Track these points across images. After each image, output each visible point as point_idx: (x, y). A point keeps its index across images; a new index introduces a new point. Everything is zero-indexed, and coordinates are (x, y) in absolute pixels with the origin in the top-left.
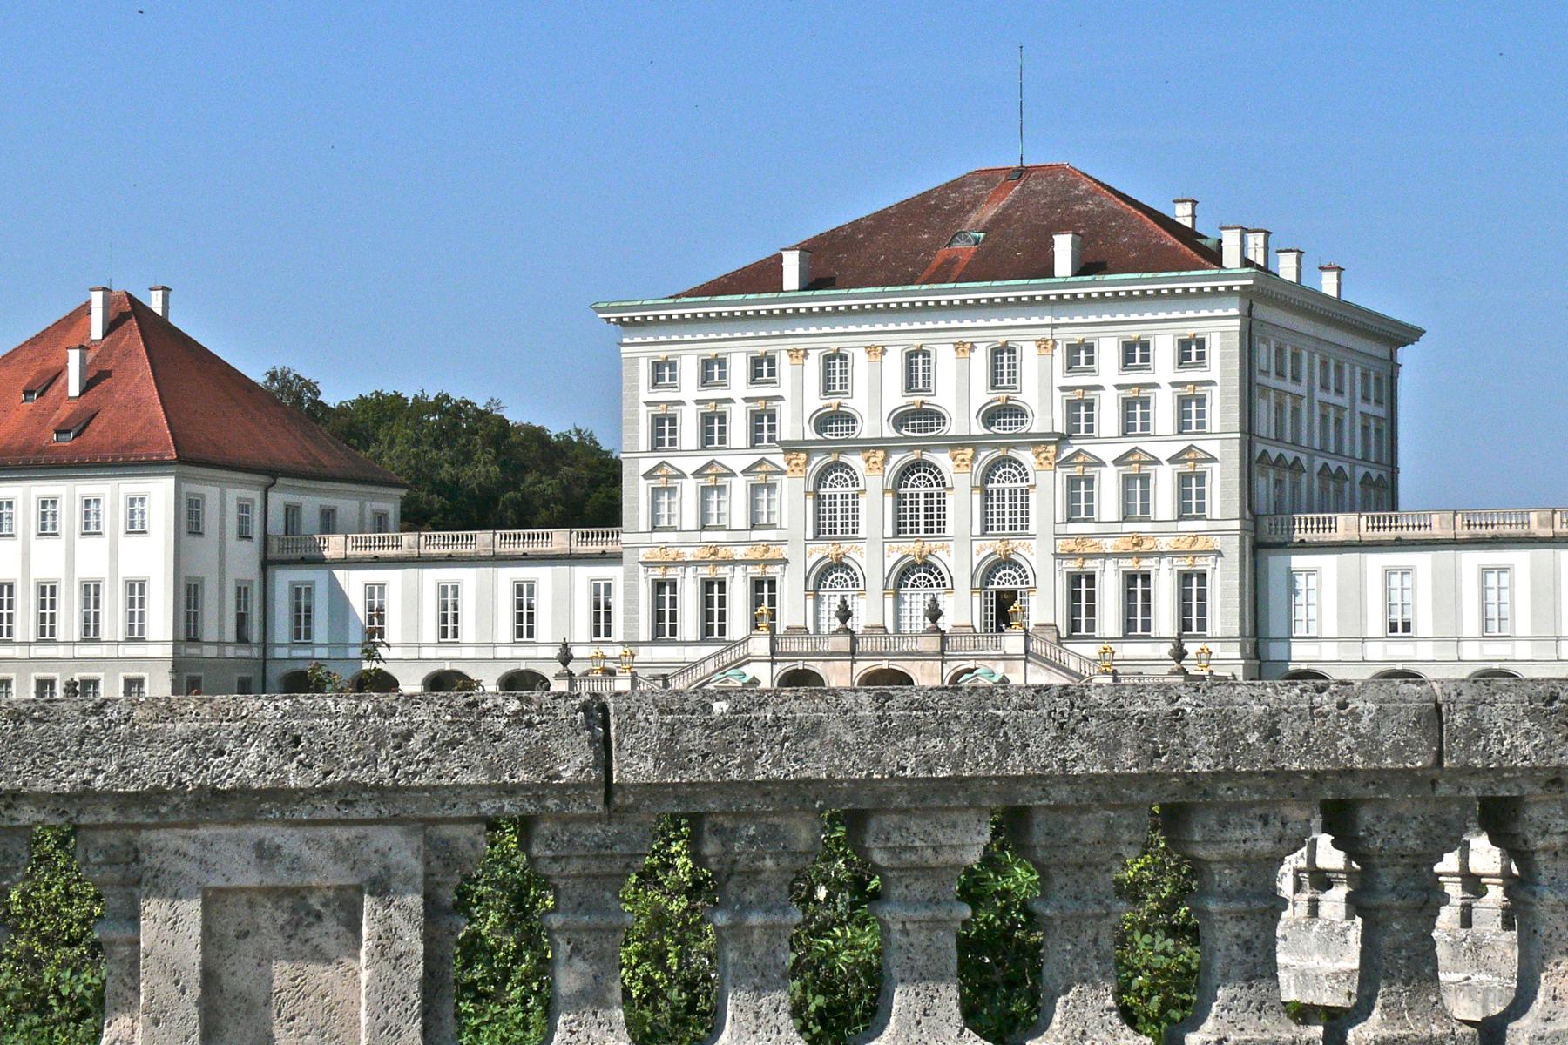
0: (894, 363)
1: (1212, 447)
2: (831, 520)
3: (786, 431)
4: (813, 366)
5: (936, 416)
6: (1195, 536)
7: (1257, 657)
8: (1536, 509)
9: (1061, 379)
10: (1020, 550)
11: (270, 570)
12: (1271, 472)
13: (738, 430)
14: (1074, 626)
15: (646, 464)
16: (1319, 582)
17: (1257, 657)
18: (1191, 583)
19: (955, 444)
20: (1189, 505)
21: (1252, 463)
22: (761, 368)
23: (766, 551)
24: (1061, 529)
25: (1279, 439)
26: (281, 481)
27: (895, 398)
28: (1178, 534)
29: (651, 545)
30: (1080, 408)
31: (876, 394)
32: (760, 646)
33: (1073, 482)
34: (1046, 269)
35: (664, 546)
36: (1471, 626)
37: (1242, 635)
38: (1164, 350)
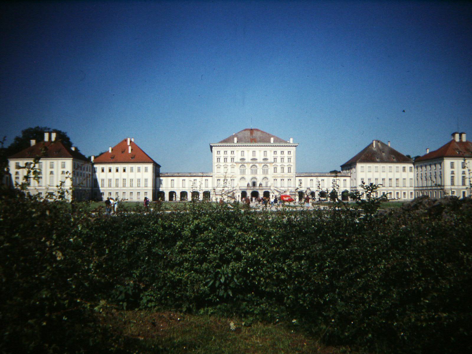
0: (251, 152)
2: (243, 172)
3: (236, 160)
4: (240, 152)
5: (256, 159)
6: (290, 175)
13: (229, 160)
15: (216, 164)
19: (260, 163)
20: (289, 171)
22: (232, 152)
30: (275, 159)
31: (248, 156)
34: (269, 142)
35: (219, 175)
38: (286, 153)
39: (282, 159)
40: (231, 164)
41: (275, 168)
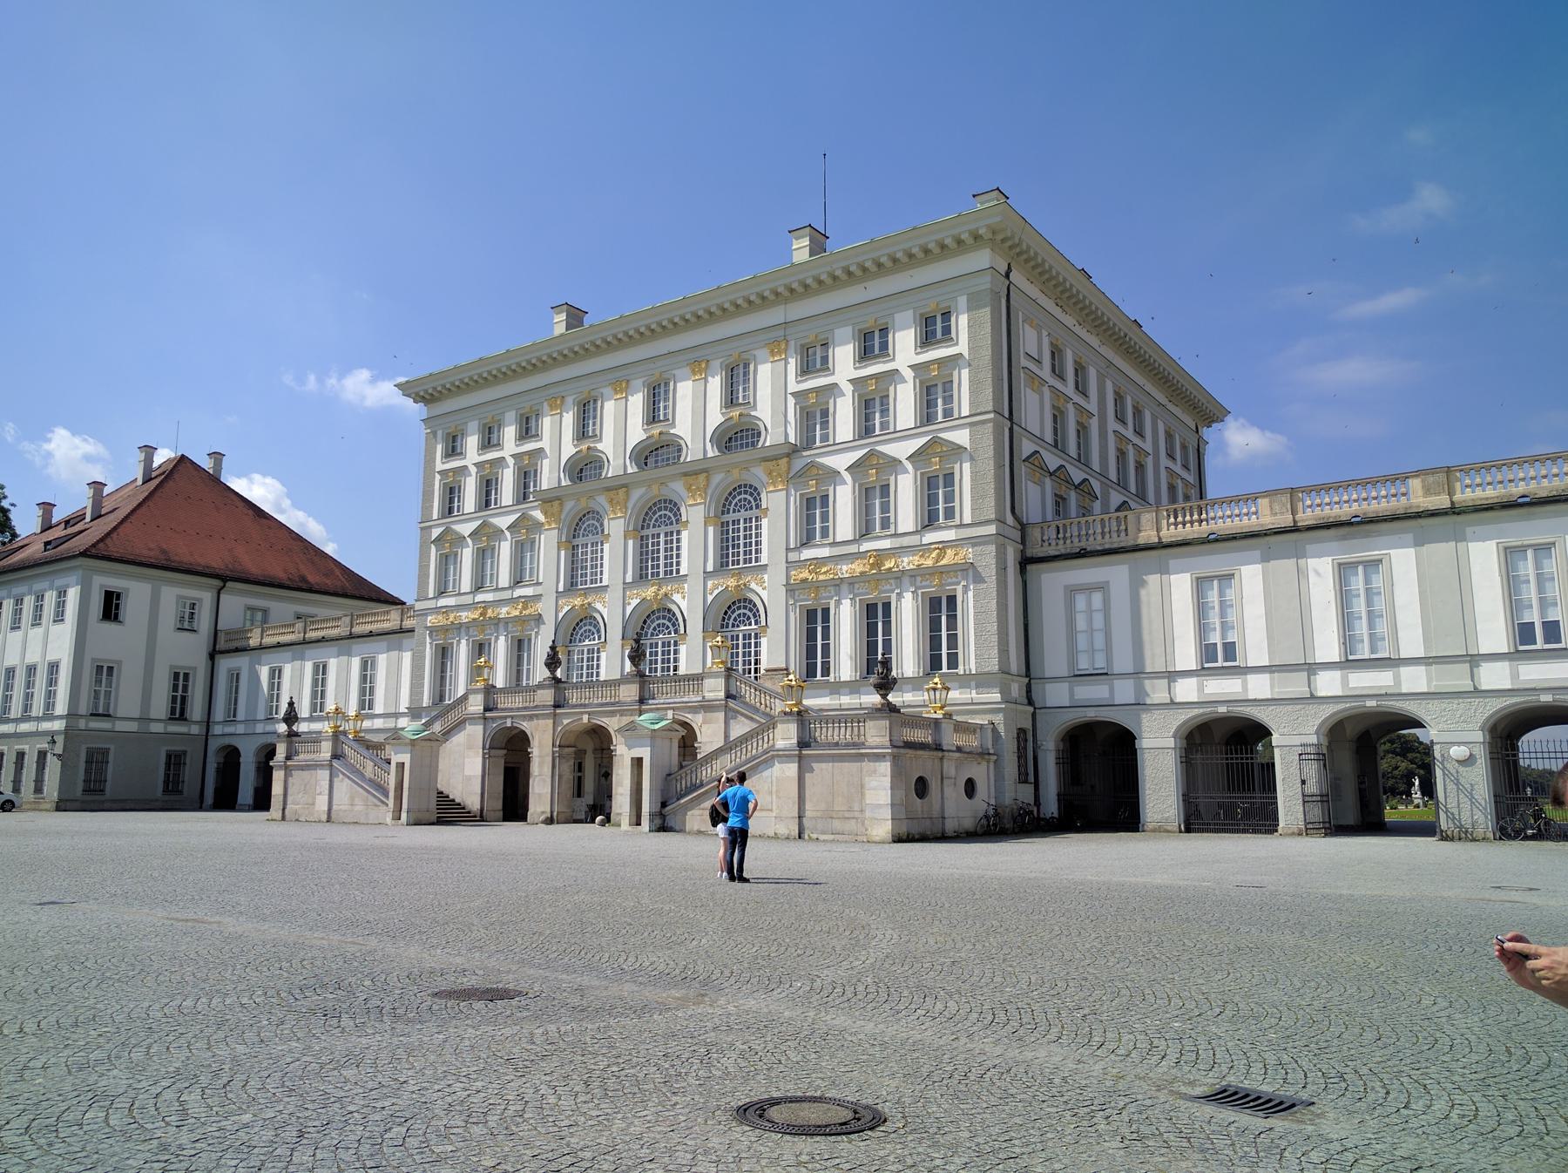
1: (961, 437)
6: (943, 546)
7: (1030, 702)
8: (1417, 474)
9: (793, 387)
10: (753, 586)
11: (217, 657)
12: (1048, 481)
14: (810, 672)
16: (1106, 602)
17: (1030, 702)
18: (941, 611)
21: (1013, 465)
23: (525, 608)
24: (793, 556)
25: (1058, 445)
26: (229, 584)
27: (637, 433)
28: (924, 550)
29: (437, 610)
30: (814, 414)
32: (476, 705)
33: (809, 503)
36: (1328, 647)
37: (1004, 671)
39: (872, 404)
40: (512, 518)
41: (814, 508)
